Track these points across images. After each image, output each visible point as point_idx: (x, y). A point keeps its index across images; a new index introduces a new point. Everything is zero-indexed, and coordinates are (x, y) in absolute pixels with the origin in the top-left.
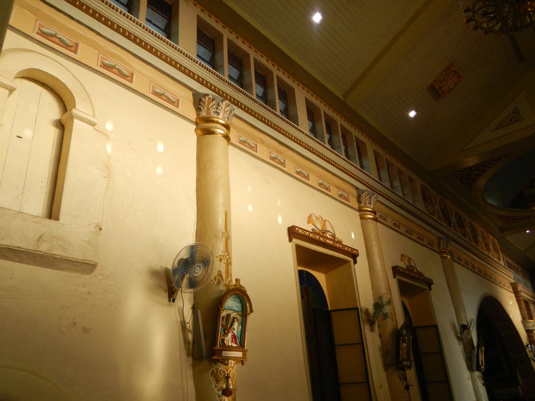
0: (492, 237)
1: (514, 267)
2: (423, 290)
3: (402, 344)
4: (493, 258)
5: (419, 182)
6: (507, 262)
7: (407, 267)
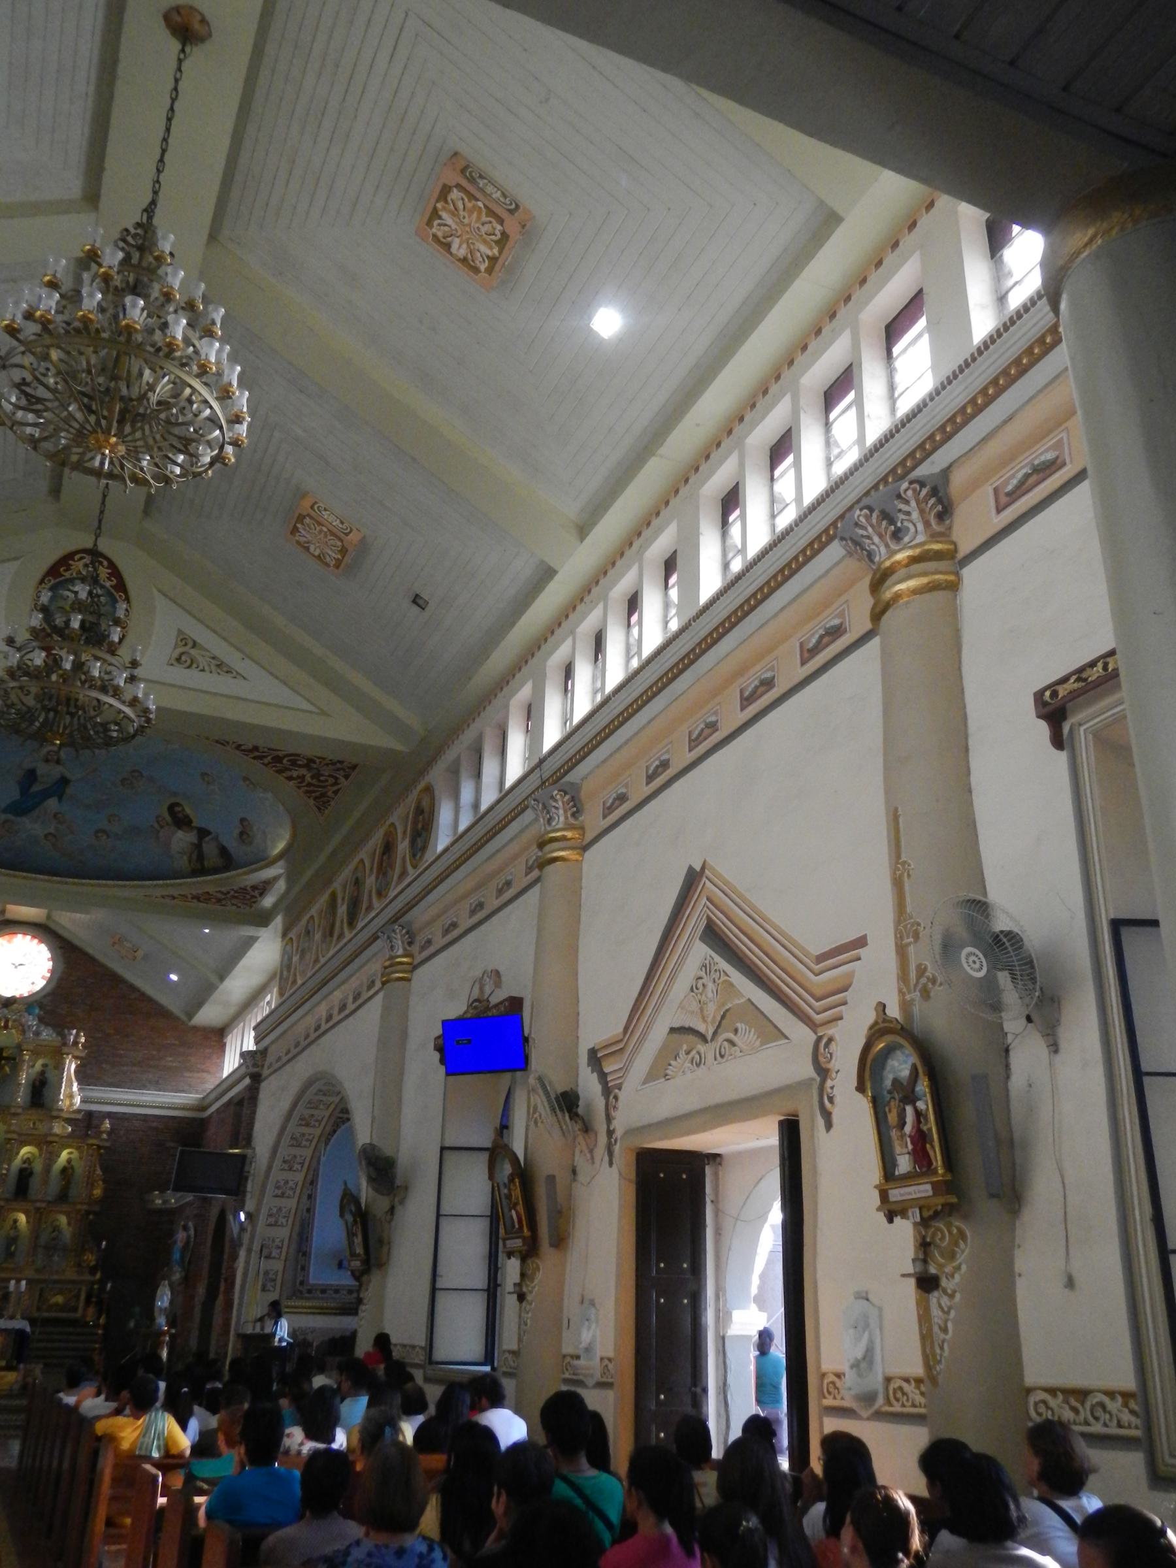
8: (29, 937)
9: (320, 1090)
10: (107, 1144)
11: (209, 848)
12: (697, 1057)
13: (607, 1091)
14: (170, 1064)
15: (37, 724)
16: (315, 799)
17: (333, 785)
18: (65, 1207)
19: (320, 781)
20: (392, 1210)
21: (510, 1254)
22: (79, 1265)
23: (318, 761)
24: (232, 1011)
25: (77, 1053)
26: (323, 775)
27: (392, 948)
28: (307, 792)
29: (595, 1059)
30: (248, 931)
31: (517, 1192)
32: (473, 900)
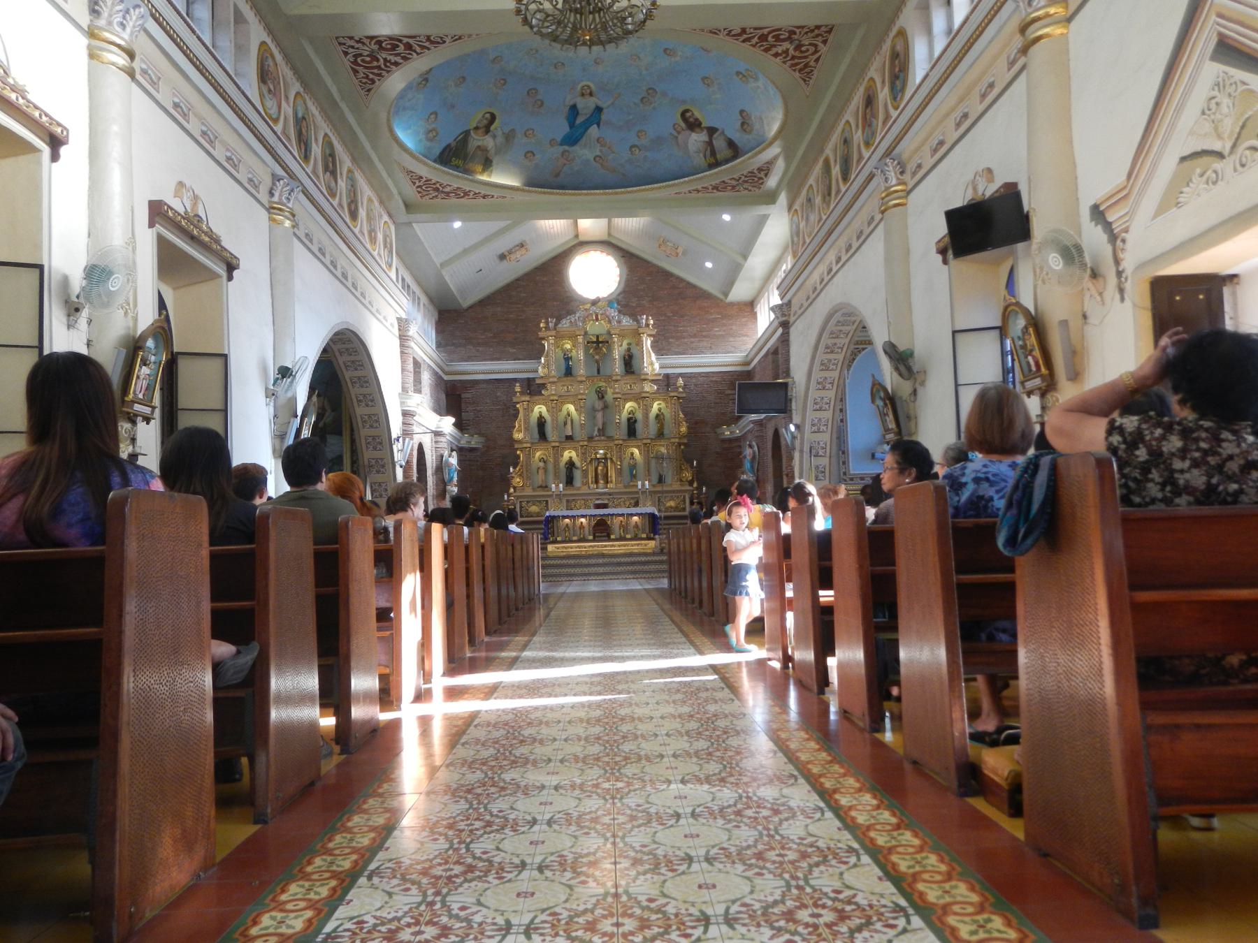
0: (386, 218)
1: (414, 293)
2: (214, 276)
3: (140, 367)
4: (377, 258)
5: (257, 34)
6: (403, 280)
7: (186, 212)
8: (598, 253)
9: (839, 322)
11: (719, 143)
12: (1214, 175)
13: (1113, 238)
15: (570, 25)
16: (800, 71)
17: (813, 54)
19: (801, 52)
20: (915, 392)
21: (1029, 394)
22: (681, 481)
23: (798, 31)
24: (757, 285)
25: (649, 333)
26: (803, 45)
27: (886, 180)
28: (792, 65)
29: (1098, 213)
30: (762, 210)
31: (1032, 340)
32: (957, 114)
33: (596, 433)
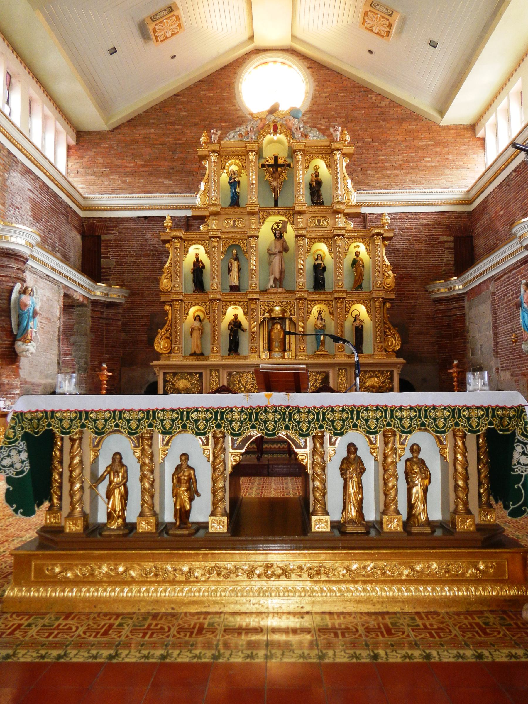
10: (392, 235)
14: (429, 164)
18: (362, 296)
22: (386, 351)
25: (344, 151)
33: (271, 283)
